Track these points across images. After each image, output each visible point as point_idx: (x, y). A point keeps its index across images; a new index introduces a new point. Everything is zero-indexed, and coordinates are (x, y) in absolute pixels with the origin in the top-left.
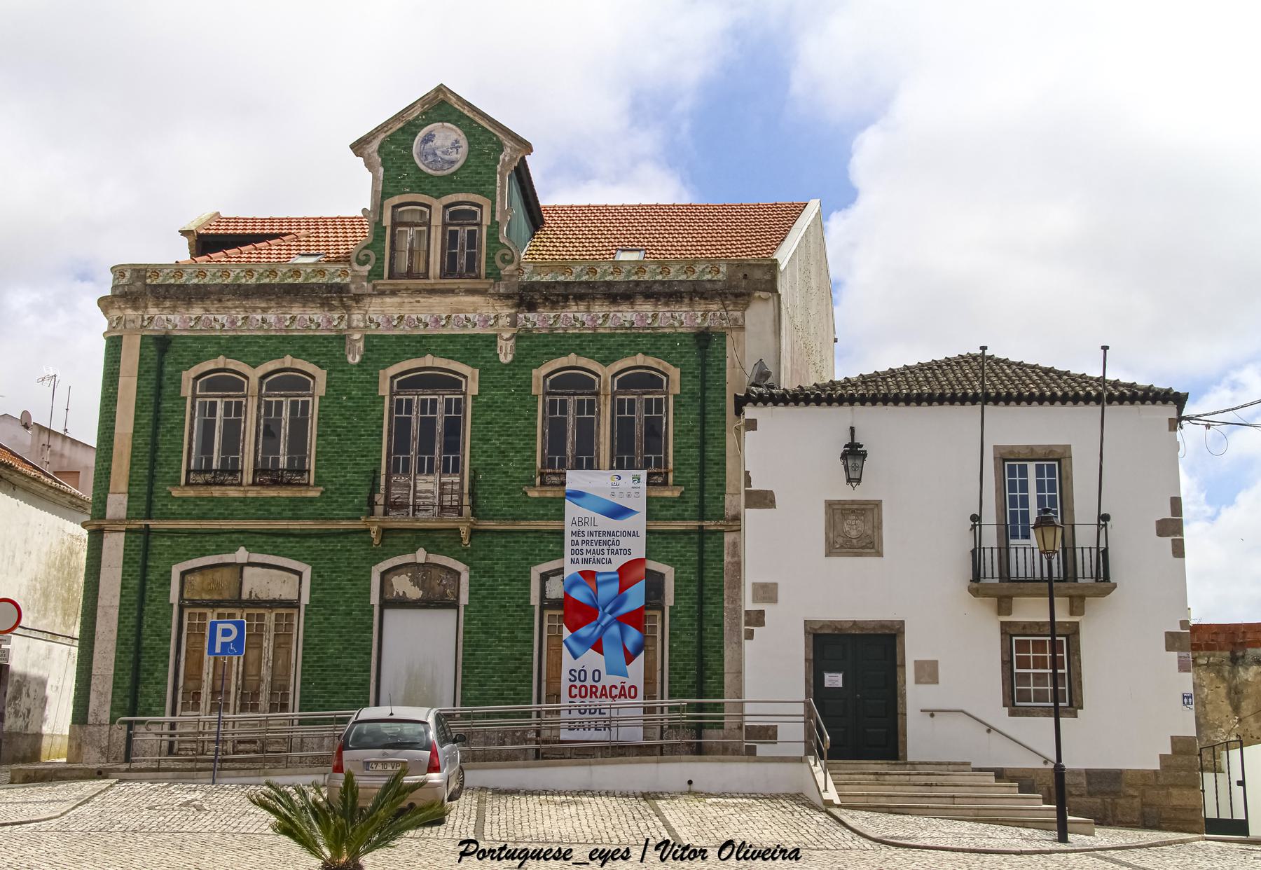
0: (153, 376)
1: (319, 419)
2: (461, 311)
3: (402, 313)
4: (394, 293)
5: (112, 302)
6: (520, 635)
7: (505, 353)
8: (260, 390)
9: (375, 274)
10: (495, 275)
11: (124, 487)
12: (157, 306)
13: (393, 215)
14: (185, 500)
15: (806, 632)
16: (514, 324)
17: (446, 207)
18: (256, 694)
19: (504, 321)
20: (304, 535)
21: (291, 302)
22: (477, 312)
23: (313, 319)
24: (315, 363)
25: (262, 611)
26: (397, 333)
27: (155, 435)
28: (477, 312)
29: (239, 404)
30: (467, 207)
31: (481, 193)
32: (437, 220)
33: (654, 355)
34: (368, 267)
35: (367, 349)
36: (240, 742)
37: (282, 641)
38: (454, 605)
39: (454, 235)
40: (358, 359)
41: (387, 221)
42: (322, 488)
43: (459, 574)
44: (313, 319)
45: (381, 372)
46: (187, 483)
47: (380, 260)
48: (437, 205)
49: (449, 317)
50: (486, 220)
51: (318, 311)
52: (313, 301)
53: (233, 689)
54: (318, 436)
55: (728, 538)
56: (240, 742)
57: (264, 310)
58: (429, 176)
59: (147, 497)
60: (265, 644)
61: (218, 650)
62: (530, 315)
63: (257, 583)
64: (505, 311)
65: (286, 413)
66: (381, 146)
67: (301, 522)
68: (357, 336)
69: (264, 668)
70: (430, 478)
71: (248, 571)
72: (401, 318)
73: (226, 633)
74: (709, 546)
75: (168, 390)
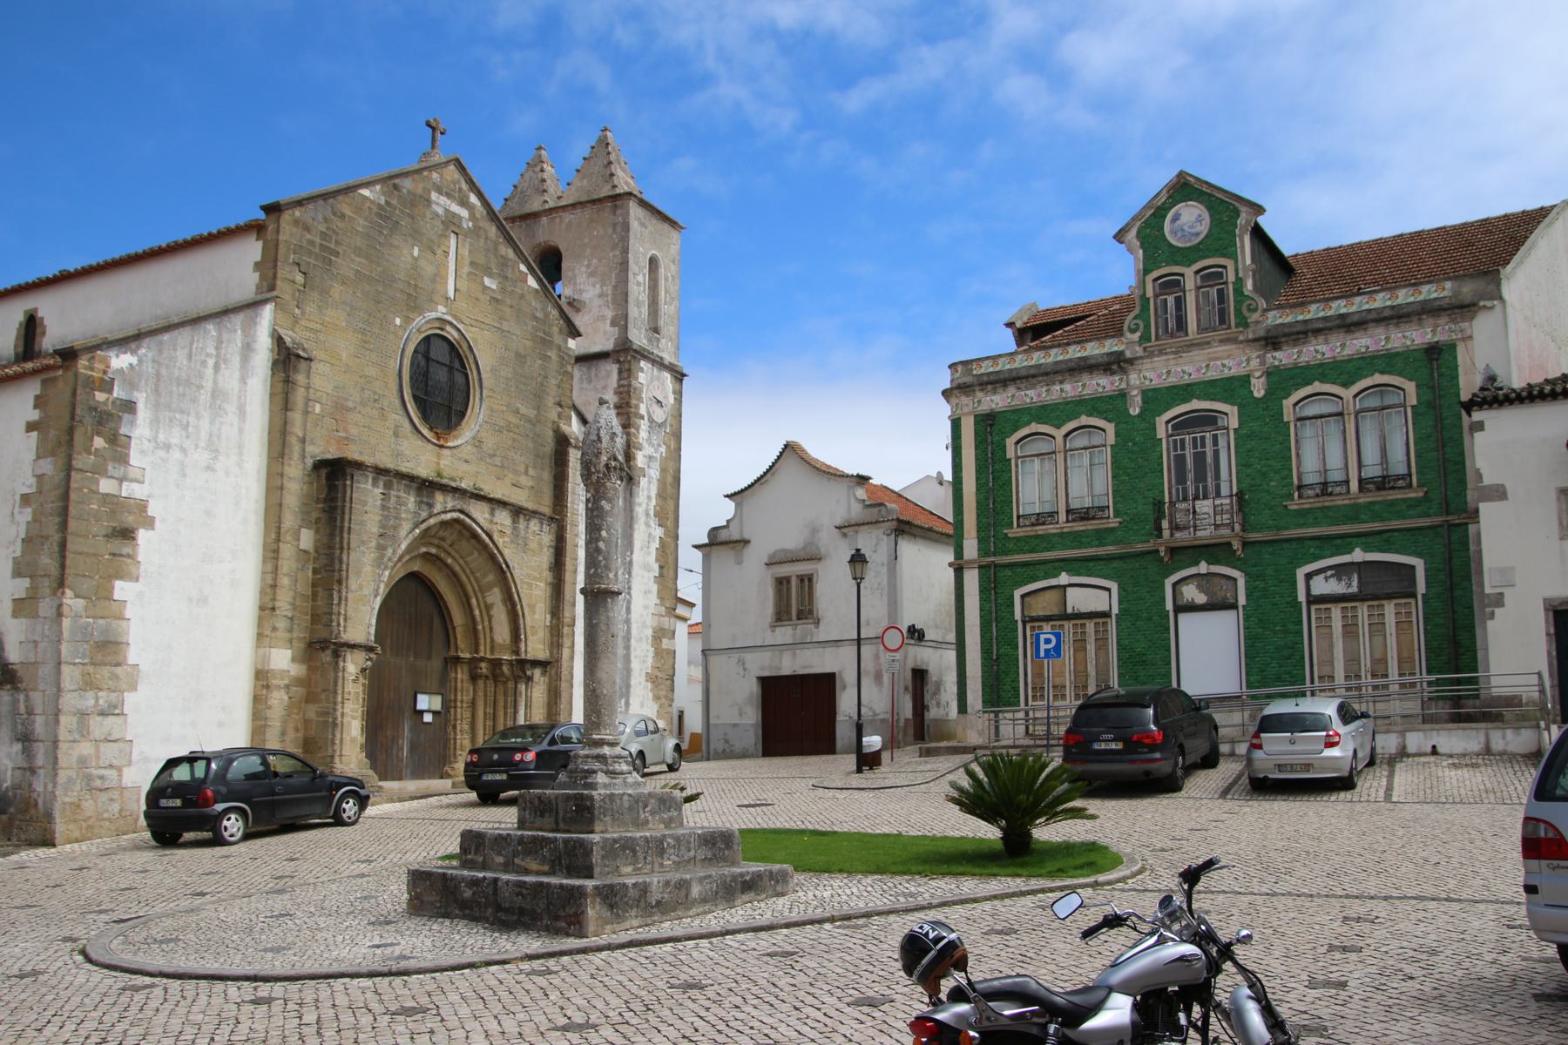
4: (1161, 353)
6: (1291, 627)
7: (1258, 389)
9: (1145, 338)
10: (1243, 323)
11: (974, 534)
14: (1018, 539)
16: (1263, 363)
17: (1197, 272)
19: (1255, 363)
20: (1110, 558)
23: (1101, 384)
31: (1224, 256)
32: (1190, 283)
33: (1390, 373)
34: (1138, 334)
35: (1144, 402)
37: (1101, 643)
38: (1234, 606)
40: (1138, 411)
43: (1235, 580)
44: (1101, 384)
47: (1147, 326)
48: (1189, 272)
50: (1231, 278)
55: (1472, 528)
62: (1277, 354)
63: (1079, 600)
68: (1135, 392)
70: (1205, 502)
73: (1048, 641)
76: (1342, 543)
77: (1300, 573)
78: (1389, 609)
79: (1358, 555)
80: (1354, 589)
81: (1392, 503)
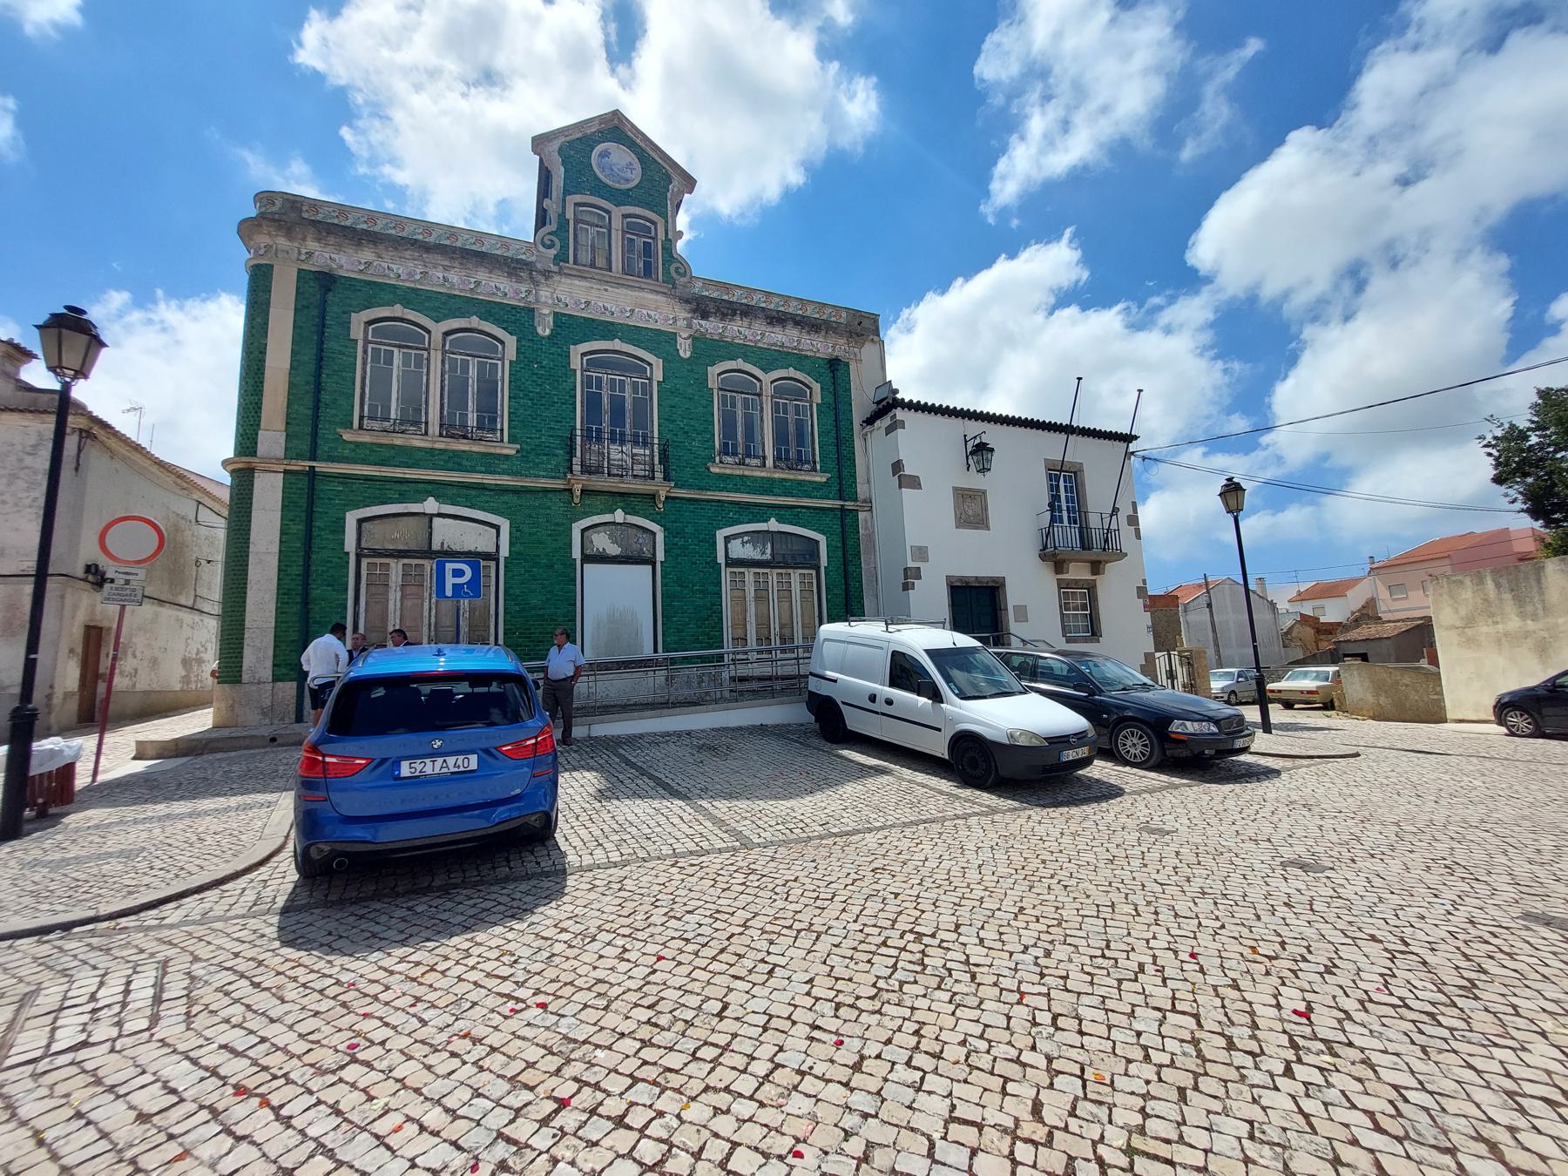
2: (643, 307)
5: (260, 225)
6: (710, 588)
12: (319, 240)
14: (358, 444)
15: (993, 579)
16: (689, 326)
19: (682, 323)
29: (419, 358)
34: (553, 252)
38: (651, 562)
40: (548, 332)
43: (654, 534)
46: (361, 427)
47: (565, 247)
50: (661, 236)
51: (502, 279)
55: (861, 516)
61: (449, 592)
63: (447, 534)
64: (682, 314)
65: (473, 372)
68: (546, 311)
71: (436, 521)
72: (588, 303)
73: (458, 573)
74: (848, 520)
76: (760, 513)
77: (720, 535)
78: (795, 576)
79: (773, 525)
80: (768, 556)
81: (800, 483)
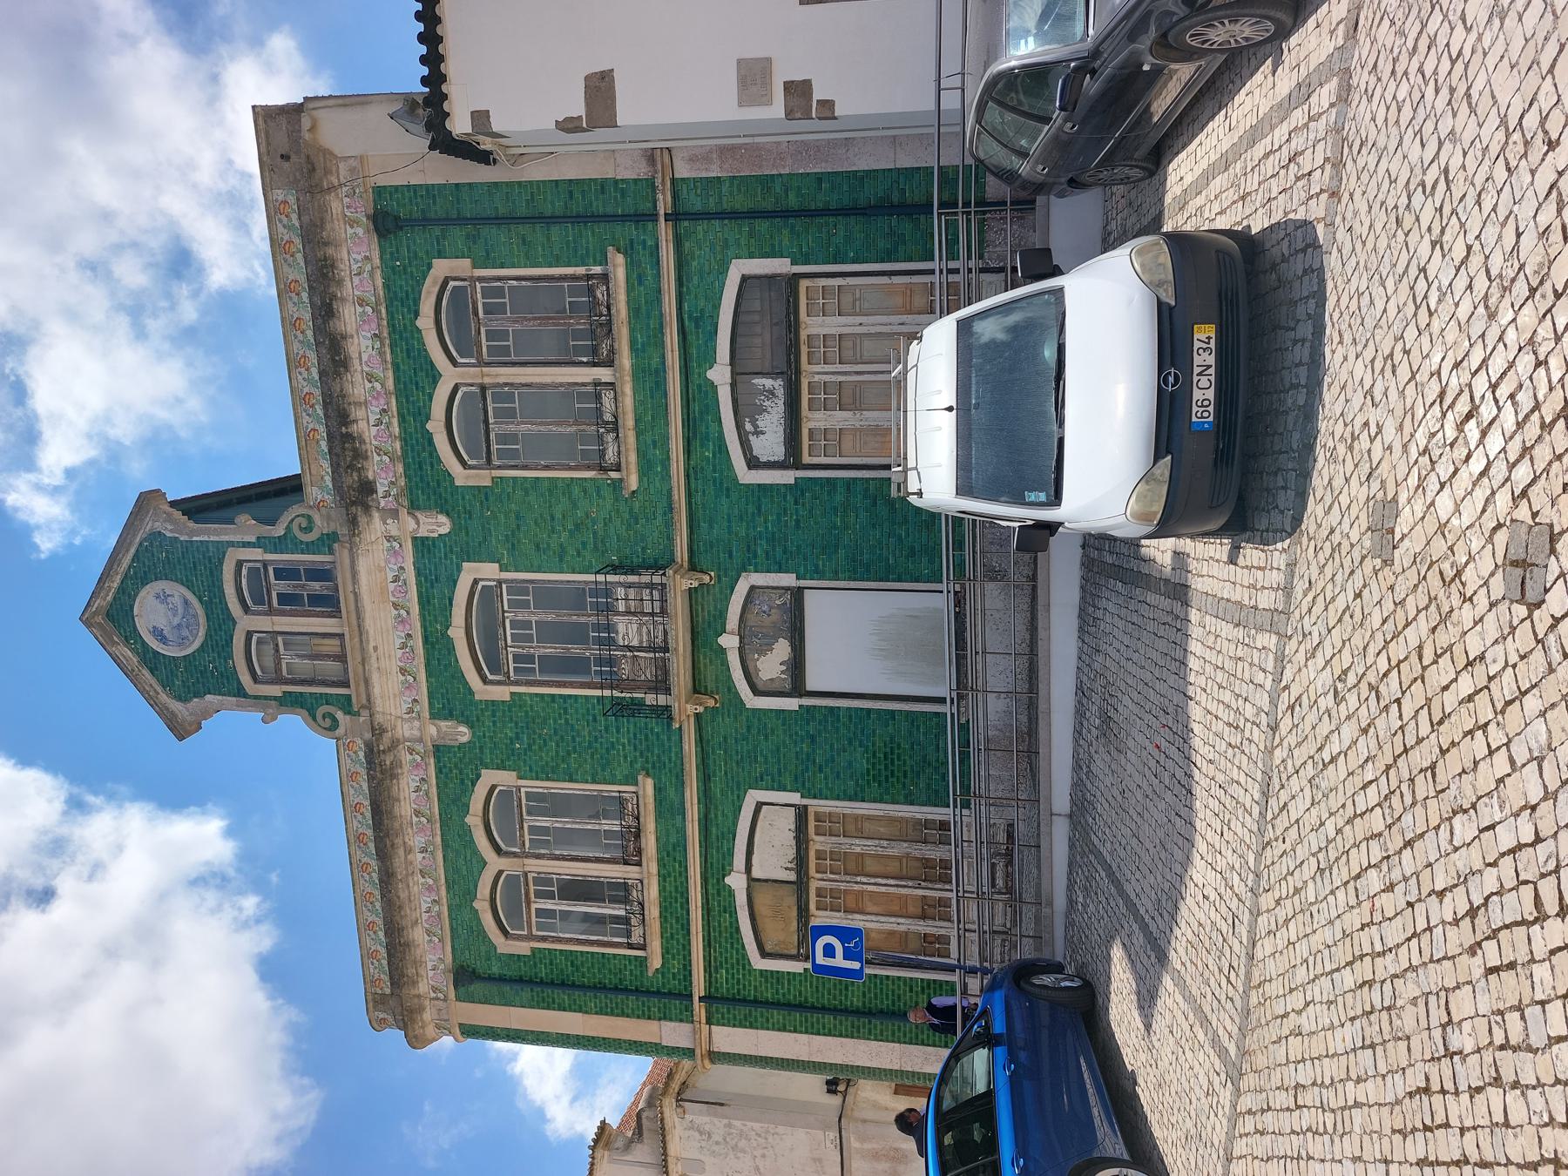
0: (507, 988)
1: (548, 779)
2: (384, 590)
3: (395, 669)
4: (367, 682)
5: (416, 1037)
6: (839, 498)
7: (437, 525)
8: (515, 855)
9: (346, 704)
10: (328, 542)
11: (653, 1025)
12: (415, 983)
13: (267, 683)
14: (666, 952)
16: (394, 514)
17: (246, 609)
18: (927, 863)
19: (393, 527)
20: (706, 796)
21: (393, 817)
22: (380, 564)
23: (414, 791)
24: (474, 785)
25: (812, 854)
26: (422, 676)
27: (582, 987)
28: (380, 564)
29: (537, 881)
30: (244, 582)
31: (221, 562)
32: (263, 623)
33: (417, 301)
34: (339, 715)
35: (450, 716)
36: (994, 886)
37: (856, 828)
38: (798, 594)
39: (283, 599)
40: (463, 729)
41: (276, 690)
42: (640, 778)
43: (753, 588)
44: (414, 791)
45: (477, 697)
46: (643, 947)
47: (328, 699)
48: (245, 623)
49: (395, 606)
51: (403, 783)
52: (389, 789)
53: (920, 892)
54: (571, 781)
55: (683, 171)
56: (994, 886)
57: (408, 851)
58: (208, 635)
59: (667, 997)
60: (858, 850)
61: (856, 965)
62: (381, 490)
63: (774, 859)
64: (375, 528)
65: (543, 822)
66: (179, 699)
67: (688, 805)
69: (890, 852)
70: (621, 628)
71: (757, 873)
72: (403, 671)
73: (829, 951)
74: (695, 203)
75: (525, 971)
76: (699, 399)
77: (746, 476)
78: (813, 325)
79: (720, 374)
80: (777, 385)
81: (635, 312)
